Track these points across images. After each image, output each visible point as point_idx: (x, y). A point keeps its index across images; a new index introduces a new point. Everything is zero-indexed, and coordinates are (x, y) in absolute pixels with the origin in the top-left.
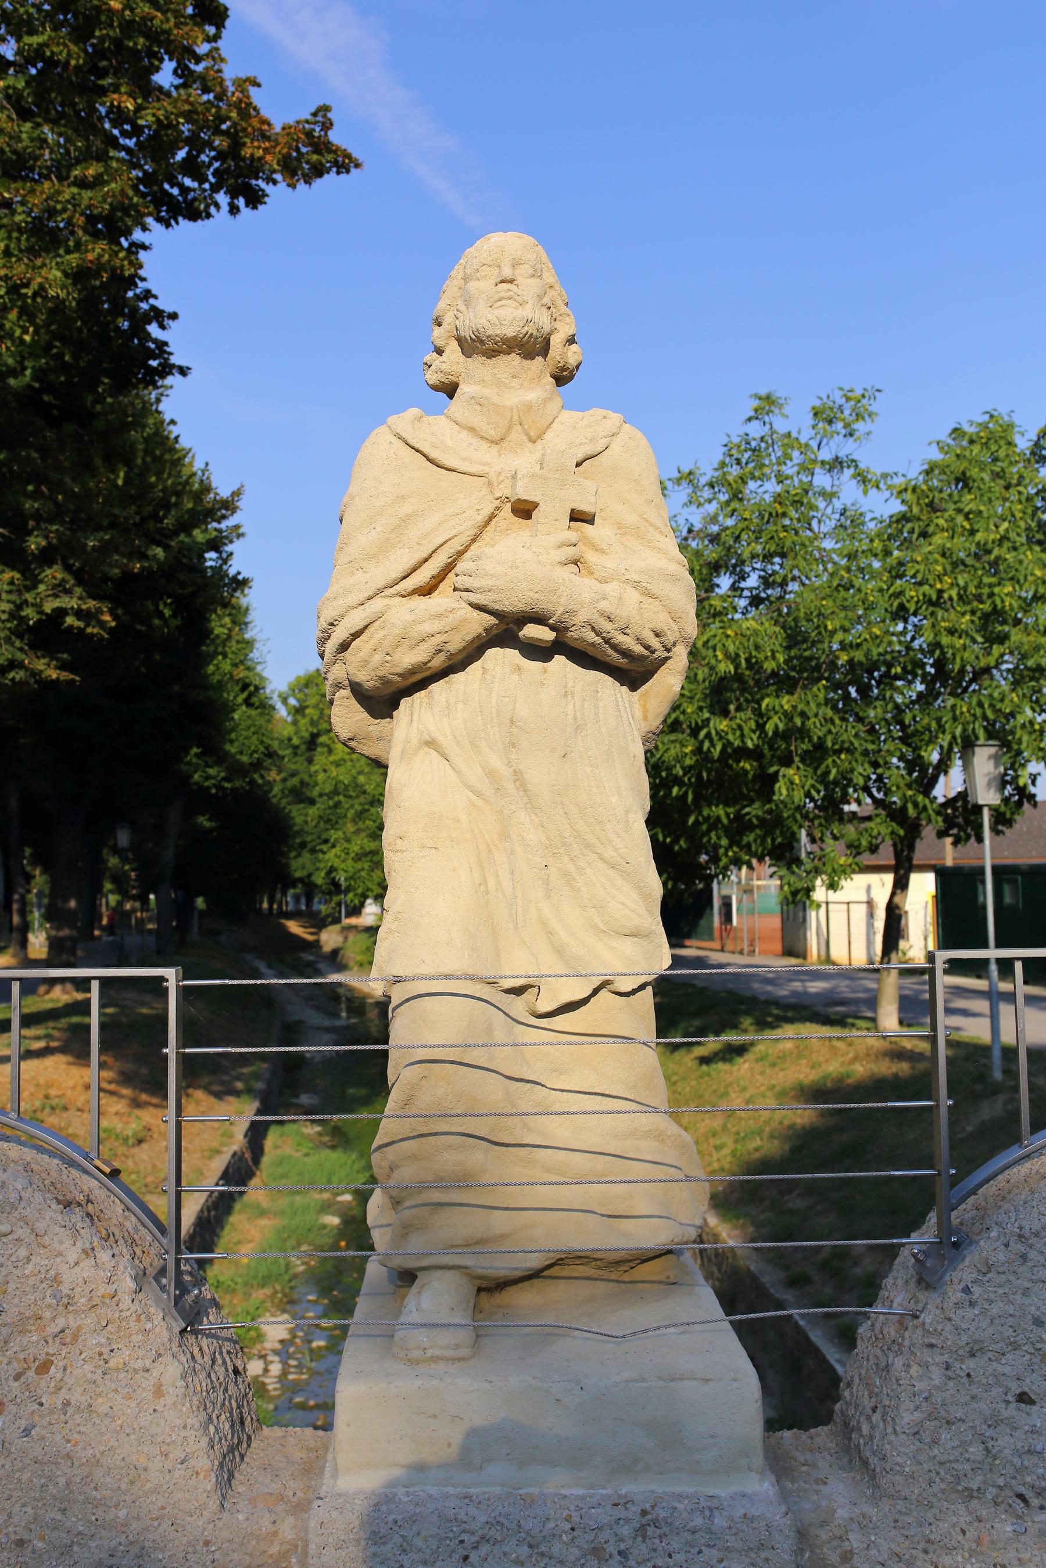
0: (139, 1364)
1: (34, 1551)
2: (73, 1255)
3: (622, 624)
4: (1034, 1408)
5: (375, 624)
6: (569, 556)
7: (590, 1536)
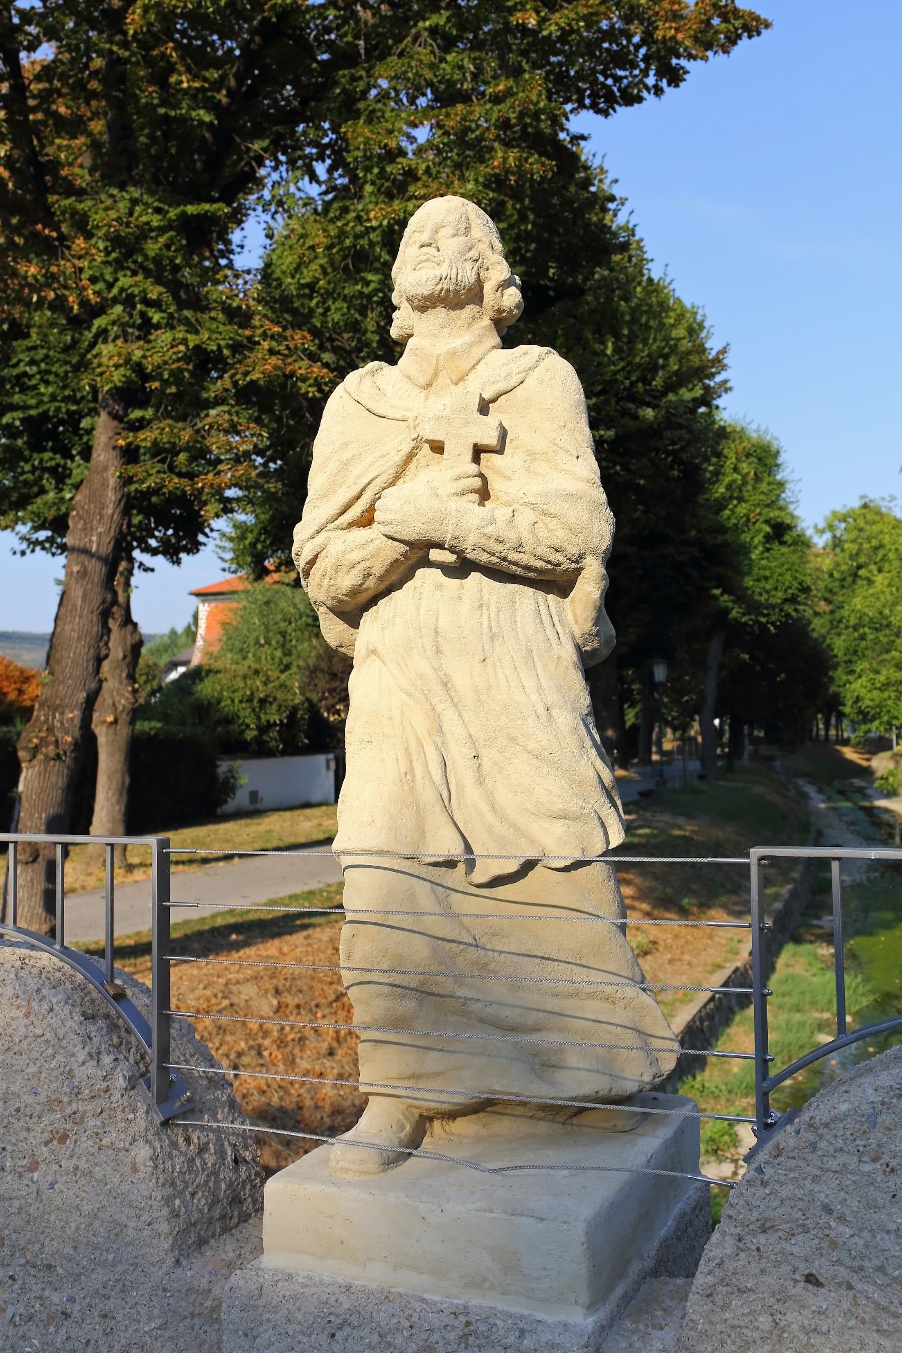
0: (122, 1145)
1: (58, 1275)
2: (81, 1057)
3: (513, 543)
4: (822, 1290)
5: (322, 554)
6: (466, 487)
7: (424, 1336)
